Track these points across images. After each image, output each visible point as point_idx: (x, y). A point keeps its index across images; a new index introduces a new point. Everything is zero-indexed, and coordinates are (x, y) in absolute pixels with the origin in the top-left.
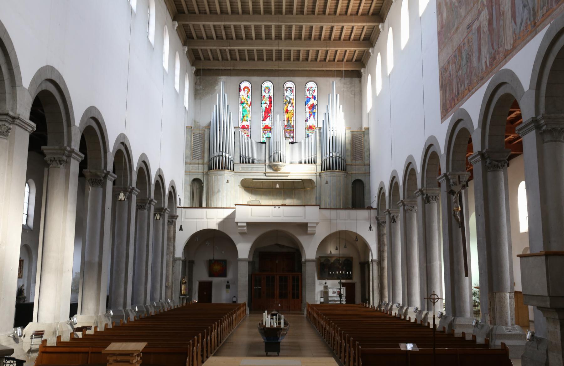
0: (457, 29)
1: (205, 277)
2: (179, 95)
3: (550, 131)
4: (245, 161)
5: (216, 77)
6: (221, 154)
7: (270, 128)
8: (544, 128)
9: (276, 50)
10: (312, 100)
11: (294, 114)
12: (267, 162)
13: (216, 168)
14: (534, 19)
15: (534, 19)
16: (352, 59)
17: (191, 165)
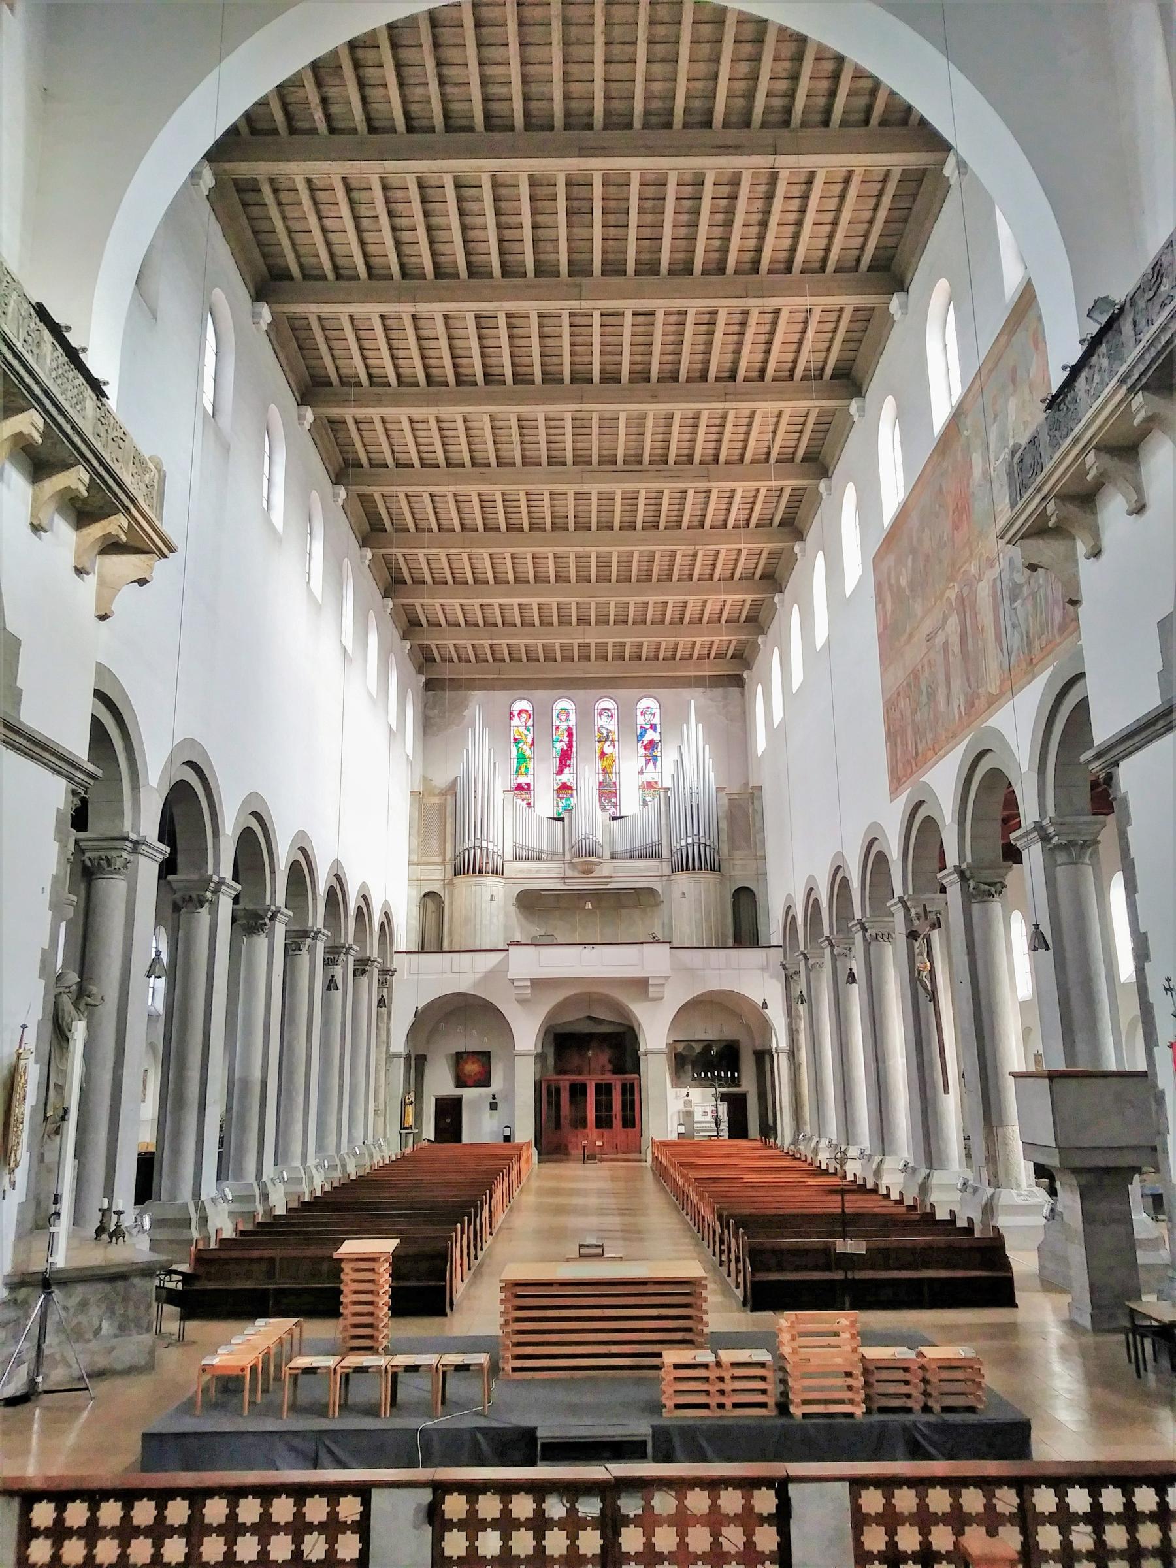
0: (911, 636)
1: (449, 1089)
2: (395, 734)
3: (1065, 847)
7: (570, 788)
8: (1055, 840)
12: (568, 856)
14: (1030, 652)
15: (1030, 652)
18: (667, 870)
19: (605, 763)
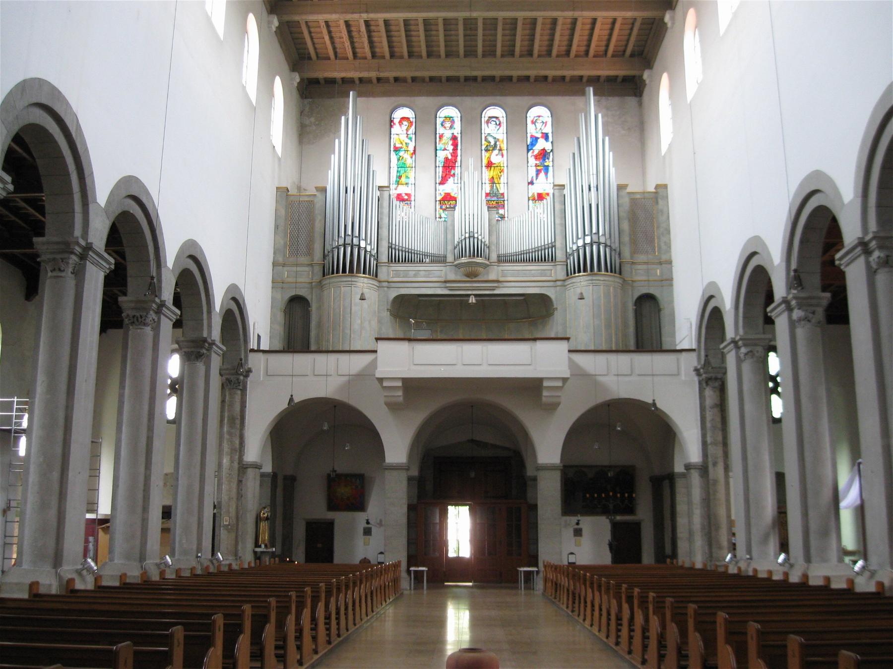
1: (321, 513)
2: (257, 112)
5: (342, 99)
6: (348, 240)
7: (455, 199)
13: (338, 272)
16: (624, 51)
17: (286, 268)
18: (559, 272)
19: (493, 173)
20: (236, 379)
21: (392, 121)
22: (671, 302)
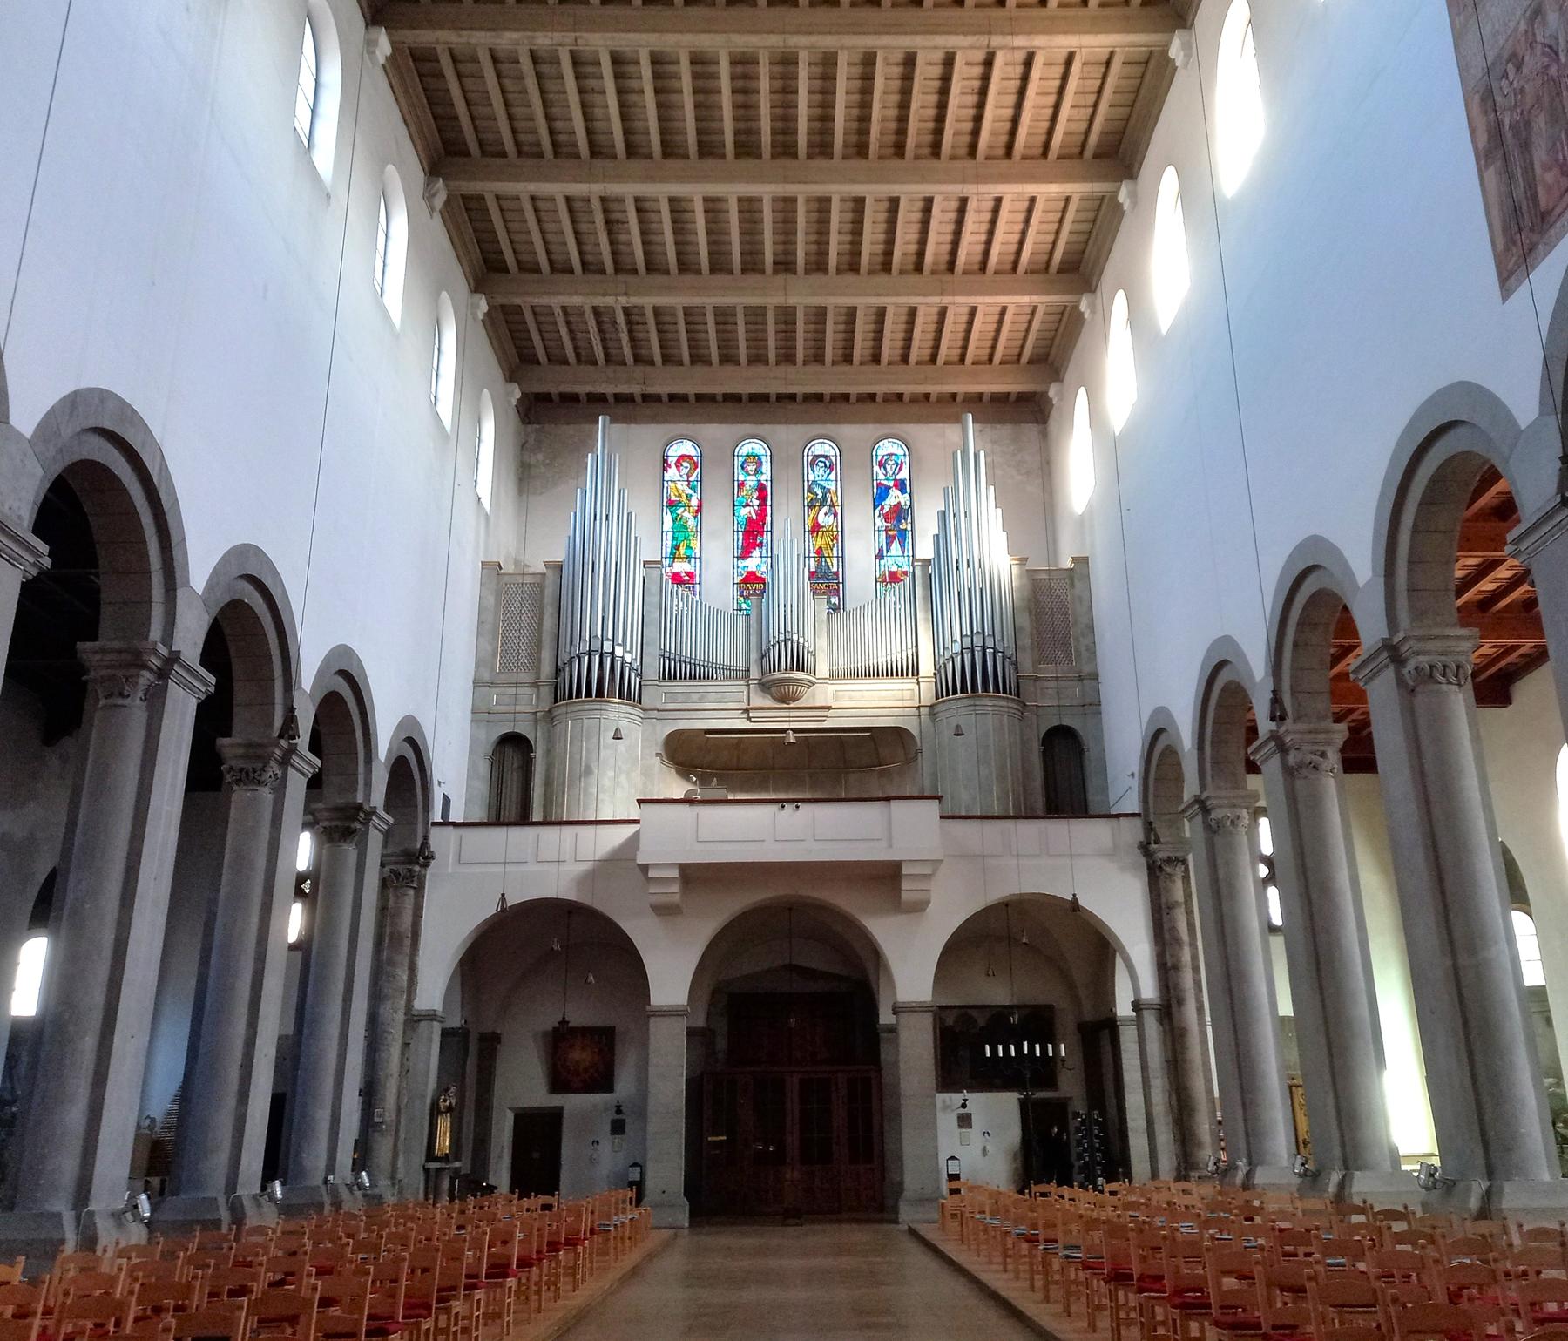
4: (676, 670)
7: (762, 581)
9: (775, 200)
10: (895, 492)
11: (837, 536)
12: (755, 673)
16: (1020, 355)
20: (408, 866)
21: (665, 461)
22: (1099, 739)
